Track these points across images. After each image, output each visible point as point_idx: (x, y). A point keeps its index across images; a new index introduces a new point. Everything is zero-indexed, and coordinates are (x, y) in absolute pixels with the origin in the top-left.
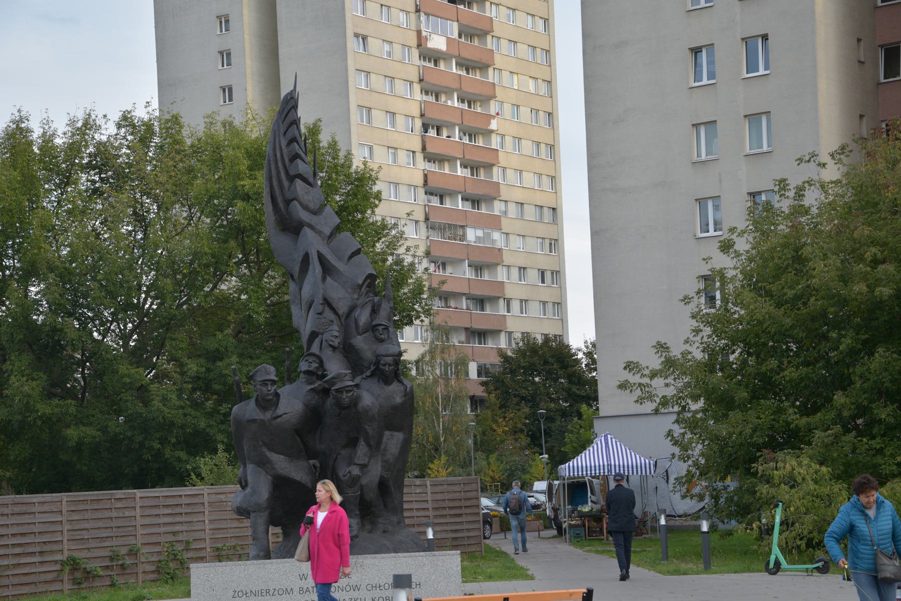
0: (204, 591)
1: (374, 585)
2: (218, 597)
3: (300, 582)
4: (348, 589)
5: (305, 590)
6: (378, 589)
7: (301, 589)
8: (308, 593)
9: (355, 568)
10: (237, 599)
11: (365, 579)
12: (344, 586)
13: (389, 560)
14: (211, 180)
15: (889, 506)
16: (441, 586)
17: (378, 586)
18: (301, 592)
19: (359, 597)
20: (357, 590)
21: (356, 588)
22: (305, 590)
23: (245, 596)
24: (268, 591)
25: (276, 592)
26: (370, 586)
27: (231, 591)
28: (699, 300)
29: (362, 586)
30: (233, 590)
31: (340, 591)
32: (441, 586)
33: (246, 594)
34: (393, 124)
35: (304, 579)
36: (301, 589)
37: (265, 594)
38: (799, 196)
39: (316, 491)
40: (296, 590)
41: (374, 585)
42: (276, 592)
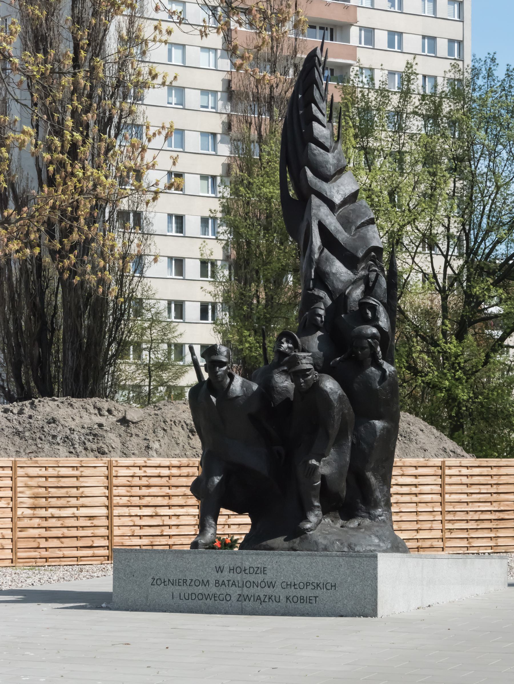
0: (125, 576)
1: (289, 583)
2: (138, 583)
3: (216, 574)
4: (263, 585)
5: (220, 583)
6: (293, 587)
7: (217, 582)
8: (223, 586)
9: (270, 564)
10: (156, 586)
11: (281, 576)
12: (259, 582)
13: (305, 558)
14: (82, 146)
15: (282, 382)
16: (357, 589)
17: (293, 584)
18: (217, 585)
19: (274, 594)
20: (271, 587)
21: (271, 585)
22: (220, 583)
23: (163, 584)
24: (184, 582)
25: (193, 583)
26: (285, 584)
27: (150, 578)
28: (163, 262)
29: (277, 584)
30: (152, 577)
31: (255, 587)
32: (357, 589)
33: (164, 582)
34: (181, 102)
35: (220, 572)
36: (217, 582)
37: (181, 584)
38: (414, 174)
39: (201, 463)
40: (212, 582)
41: (289, 583)
42: (193, 583)
